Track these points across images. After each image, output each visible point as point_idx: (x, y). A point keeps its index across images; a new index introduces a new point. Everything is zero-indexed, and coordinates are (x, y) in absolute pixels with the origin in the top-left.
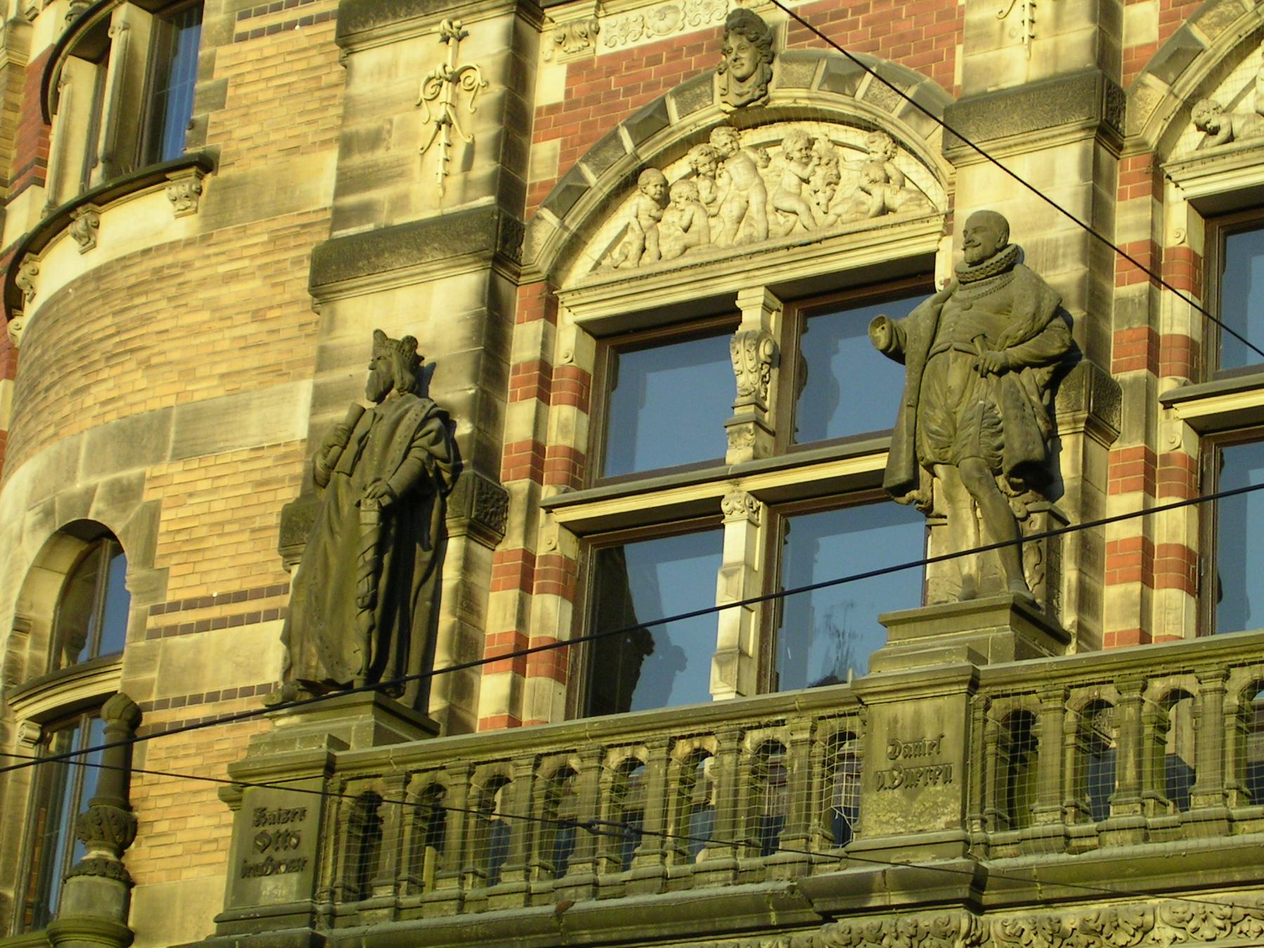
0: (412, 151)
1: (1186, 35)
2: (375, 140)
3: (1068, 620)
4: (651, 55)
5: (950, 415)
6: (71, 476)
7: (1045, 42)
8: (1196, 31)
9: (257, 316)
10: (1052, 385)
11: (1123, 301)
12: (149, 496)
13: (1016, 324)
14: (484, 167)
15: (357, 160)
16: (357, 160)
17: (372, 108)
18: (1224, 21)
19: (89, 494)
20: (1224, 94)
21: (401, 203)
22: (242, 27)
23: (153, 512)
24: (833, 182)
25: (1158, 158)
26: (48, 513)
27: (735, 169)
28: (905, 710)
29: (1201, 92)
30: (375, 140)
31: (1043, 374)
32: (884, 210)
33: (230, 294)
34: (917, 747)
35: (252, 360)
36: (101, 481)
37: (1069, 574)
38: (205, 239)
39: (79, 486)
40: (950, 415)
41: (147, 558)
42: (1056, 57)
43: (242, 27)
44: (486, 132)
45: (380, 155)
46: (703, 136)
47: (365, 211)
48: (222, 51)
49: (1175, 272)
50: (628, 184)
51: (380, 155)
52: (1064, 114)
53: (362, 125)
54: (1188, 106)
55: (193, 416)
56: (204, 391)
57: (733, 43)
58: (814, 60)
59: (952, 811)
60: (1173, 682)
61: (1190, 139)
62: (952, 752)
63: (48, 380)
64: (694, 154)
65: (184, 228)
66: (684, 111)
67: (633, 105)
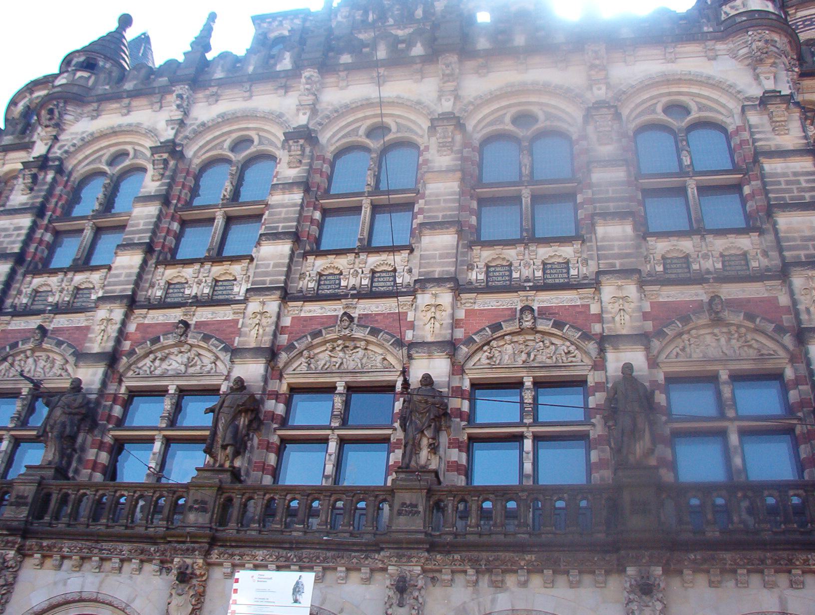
1: (134, 350)
3: (71, 475)
4: (19, 331)
5: (55, 421)
7: (103, 345)
8: (136, 349)
10: (82, 420)
11: (105, 406)
13: (76, 405)
18: (143, 348)
20: (140, 365)
24: (51, 368)
25: (121, 376)
27: (30, 360)
29: (135, 363)
31: (79, 417)
32: (61, 375)
34: (22, 497)
37: (74, 464)
40: (55, 421)
46: (24, 352)
49: (120, 401)
52: (103, 361)
54: (131, 365)
57: (37, 331)
58: (54, 339)
59: (25, 514)
60: (85, 491)
61: (130, 373)
62: (30, 500)
64: (22, 355)
66: (23, 344)
67: (12, 341)
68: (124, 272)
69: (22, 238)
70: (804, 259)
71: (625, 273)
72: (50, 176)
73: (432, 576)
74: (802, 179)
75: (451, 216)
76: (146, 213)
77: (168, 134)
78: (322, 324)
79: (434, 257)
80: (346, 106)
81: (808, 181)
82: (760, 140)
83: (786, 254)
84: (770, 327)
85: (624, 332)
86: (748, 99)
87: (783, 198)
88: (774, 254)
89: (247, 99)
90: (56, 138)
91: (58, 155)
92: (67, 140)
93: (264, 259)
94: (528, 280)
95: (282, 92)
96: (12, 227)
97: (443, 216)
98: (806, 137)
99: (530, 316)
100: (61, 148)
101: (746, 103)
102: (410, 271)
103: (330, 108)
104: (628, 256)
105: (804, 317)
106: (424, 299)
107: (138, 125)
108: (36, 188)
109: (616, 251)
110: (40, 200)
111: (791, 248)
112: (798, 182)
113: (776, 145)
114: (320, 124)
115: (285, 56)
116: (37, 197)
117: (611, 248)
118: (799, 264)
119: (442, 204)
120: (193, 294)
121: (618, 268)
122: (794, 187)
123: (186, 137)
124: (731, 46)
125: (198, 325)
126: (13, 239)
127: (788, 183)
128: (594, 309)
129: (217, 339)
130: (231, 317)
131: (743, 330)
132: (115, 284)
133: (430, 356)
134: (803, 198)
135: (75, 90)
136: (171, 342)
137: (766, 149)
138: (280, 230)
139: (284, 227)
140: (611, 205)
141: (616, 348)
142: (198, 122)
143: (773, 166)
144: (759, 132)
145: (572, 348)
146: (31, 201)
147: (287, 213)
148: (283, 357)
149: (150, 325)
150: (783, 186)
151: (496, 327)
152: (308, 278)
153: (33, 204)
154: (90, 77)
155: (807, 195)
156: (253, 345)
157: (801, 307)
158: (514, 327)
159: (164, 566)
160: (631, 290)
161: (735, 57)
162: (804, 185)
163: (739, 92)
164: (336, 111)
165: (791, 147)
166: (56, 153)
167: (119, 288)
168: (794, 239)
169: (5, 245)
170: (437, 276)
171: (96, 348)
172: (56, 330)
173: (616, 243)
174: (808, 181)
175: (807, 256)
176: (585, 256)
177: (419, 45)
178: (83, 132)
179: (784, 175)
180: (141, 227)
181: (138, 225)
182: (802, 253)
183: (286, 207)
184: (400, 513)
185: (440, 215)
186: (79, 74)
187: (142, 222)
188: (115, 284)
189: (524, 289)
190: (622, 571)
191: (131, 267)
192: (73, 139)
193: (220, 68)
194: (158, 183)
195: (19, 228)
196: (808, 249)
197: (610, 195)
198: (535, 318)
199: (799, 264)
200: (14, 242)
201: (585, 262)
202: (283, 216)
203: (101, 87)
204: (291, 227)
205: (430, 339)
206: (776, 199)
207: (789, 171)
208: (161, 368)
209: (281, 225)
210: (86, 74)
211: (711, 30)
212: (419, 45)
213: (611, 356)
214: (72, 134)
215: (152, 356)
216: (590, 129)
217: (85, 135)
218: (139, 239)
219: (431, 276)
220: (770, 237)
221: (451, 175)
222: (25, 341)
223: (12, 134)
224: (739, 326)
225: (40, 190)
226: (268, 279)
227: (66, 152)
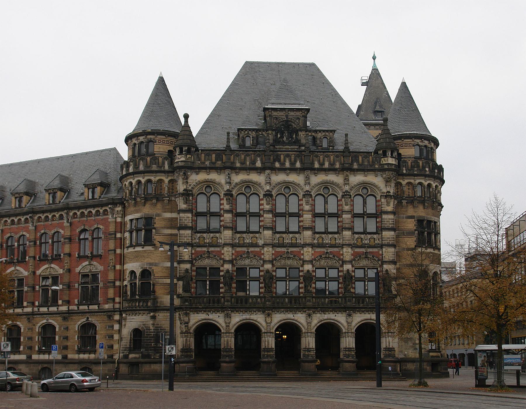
0: (185, 255)
2: (182, 254)
6: (144, 265)
9: (161, 257)
12: (153, 268)
14: (190, 257)
15: (180, 255)
16: (180, 255)
17: (181, 251)
19: (147, 268)
21: (184, 258)
22: (156, 235)
23: (153, 270)
26: (142, 268)
28: (227, 298)
30: (182, 254)
33: (158, 255)
35: (160, 260)
36: (148, 267)
38: (155, 250)
39: (145, 266)
41: (153, 273)
42: (230, 259)
43: (156, 235)
44: (190, 255)
45: (182, 255)
47: (182, 258)
48: (155, 236)
50: (200, 259)
51: (182, 255)
53: (180, 252)
55: (156, 263)
56: (156, 262)
63: (139, 257)
65: (153, 249)
68: (228, 236)
69: (191, 221)
70: (386, 244)
71: (349, 245)
72: (191, 198)
73: (314, 312)
74: (390, 220)
75: (310, 226)
76: (228, 216)
77: (227, 187)
78: (282, 253)
79: (307, 238)
80: (279, 183)
81: (391, 221)
82: (383, 207)
83: (383, 242)
84: (377, 259)
85: (348, 260)
86: (382, 193)
87: (385, 226)
88: (380, 240)
89: (248, 175)
90: (187, 183)
91: (190, 188)
92: (191, 182)
93: (265, 235)
94: (327, 244)
95: (259, 174)
96: (186, 217)
97: (308, 226)
98: (393, 208)
99: (328, 254)
100: (190, 185)
101: (382, 194)
102: (300, 239)
103: (274, 183)
104: (349, 240)
105: (384, 258)
106: (305, 249)
107: (215, 180)
108: (187, 202)
109: (347, 239)
110: (191, 207)
111: (384, 241)
112: (389, 221)
113: (387, 209)
114: (273, 189)
115: (258, 159)
116: (190, 206)
117: (346, 238)
118: (385, 245)
119: (308, 222)
120: (247, 242)
121: (347, 243)
122: (388, 223)
123: (233, 188)
124: (382, 173)
125: (251, 252)
126: (188, 221)
127: (387, 221)
128: (341, 252)
129: (257, 256)
130: (259, 250)
131: (371, 259)
132: (227, 240)
133: (308, 264)
134: (389, 226)
135: (189, 164)
136: (245, 256)
137: (384, 210)
138: (268, 226)
139: (269, 225)
140: (347, 225)
141: (346, 264)
142: (235, 182)
143: (385, 216)
144: (383, 205)
145: (336, 261)
146: (188, 207)
147: (269, 221)
148: (274, 262)
149: (238, 251)
150: (386, 223)
151: (321, 256)
152: (276, 240)
153: (189, 208)
154: (191, 156)
155: (390, 226)
156: (268, 260)
157: (384, 256)
158: (325, 256)
159: (264, 312)
160: (350, 250)
161: (382, 177)
162: (390, 222)
163: (381, 190)
164: (276, 185)
165: (390, 211)
166: (189, 188)
167: (228, 241)
168: (385, 238)
169: (186, 223)
170: (308, 243)
171: (227, 259)
172: (212, 251)
173: (347, 237)
174: (391, 221)
175: (387, 243)
176: (340, 237)
177: (298, 162)
178: (196, 180)
179: (387, 219)
180: (228, 221)
181: (227, 220)
182: (386, 242)
183: (268, 219)
184: (307, 301)
185: (307, 225)
186: (188, 156)
187: (228, 219)
188: (227, 240)
189: (326, 247)
190: (346, 312)
191: (230, 235)
192: (193, 182)
193: (237, 161)
194: (229, 206)
195: (188, 217)
196: (387, 241)
197: (347, 222)
198: (329, 255)
199: (385, 245)
200: (189, 223)
201: (340, 240)
202: (268, 221)
203: (197, 162)
204: (271, 225)
205: (307, 260)
206: (384, 226)
207: (388, 218)
208: (243, 263)
209: (268, 224)
210: (190, 156)
211: (378, 167)
212: (298, 162)
213: (344, 265)
214: (192, 180)
215: (241, 260)
216: (343, 200)
217: (197, 181)
218: (229, 225)
219: (306, 243)
220: (380, 235)
221: (309, 213)
222: (204, 254)
223: (155, 164)
224: (371, 258)
225: (190, 203)
226: (268, 241)
227: (193, 188)
